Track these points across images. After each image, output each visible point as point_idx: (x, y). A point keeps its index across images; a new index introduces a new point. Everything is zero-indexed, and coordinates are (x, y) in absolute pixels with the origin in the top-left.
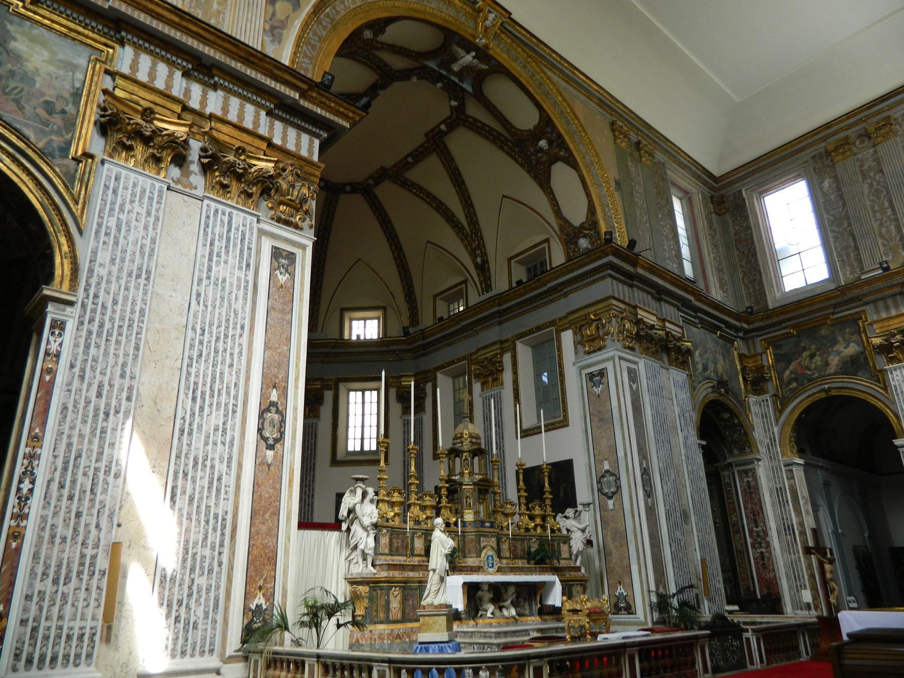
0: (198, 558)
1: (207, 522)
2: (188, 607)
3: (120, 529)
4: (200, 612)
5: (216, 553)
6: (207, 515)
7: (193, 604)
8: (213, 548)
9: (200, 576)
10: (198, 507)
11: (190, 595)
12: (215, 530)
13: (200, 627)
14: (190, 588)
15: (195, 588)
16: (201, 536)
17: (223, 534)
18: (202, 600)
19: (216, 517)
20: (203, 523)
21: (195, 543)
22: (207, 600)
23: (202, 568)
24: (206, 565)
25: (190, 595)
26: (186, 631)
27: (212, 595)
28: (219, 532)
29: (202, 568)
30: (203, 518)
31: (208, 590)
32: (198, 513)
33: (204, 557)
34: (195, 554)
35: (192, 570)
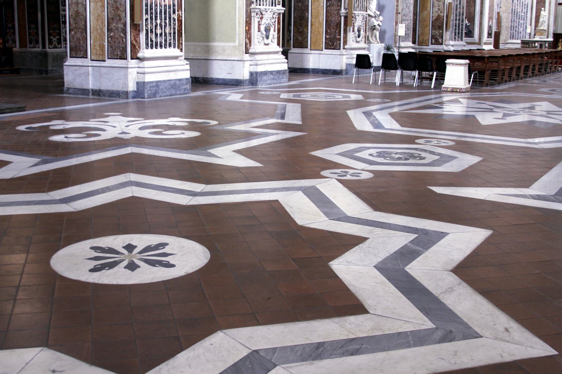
0: (520, 15)
1: (522, 6)
2: (518, 28)
3: (501, 9)
4: (522, 29)
5: (525, 14)
6: (522, 4)
7: (520, 27)
8: (524, 13)
9: (521, 20)
10: (520, 2)
11: (519, 25)
12: (525, 8)
13: (522, 33)
14: (519, 23)
15: (520, 23)
16: (521, 10)
17: (527, 9)
18: (522, 26)
19: (525, 4)
20: (521, 7)
21: (520, 12)
22: (523, 27)
23: (522, 18)
24: (523, 17)
25: (519, 25)
26: (518, 34)
27: (525, 25)
28: (526, 9)
29: (522, 18)
30: (521, 5)
31: (524, 24)
32: (520, 4)
33: (522, 15)
34: (519, 15)
35: (519, 19)
